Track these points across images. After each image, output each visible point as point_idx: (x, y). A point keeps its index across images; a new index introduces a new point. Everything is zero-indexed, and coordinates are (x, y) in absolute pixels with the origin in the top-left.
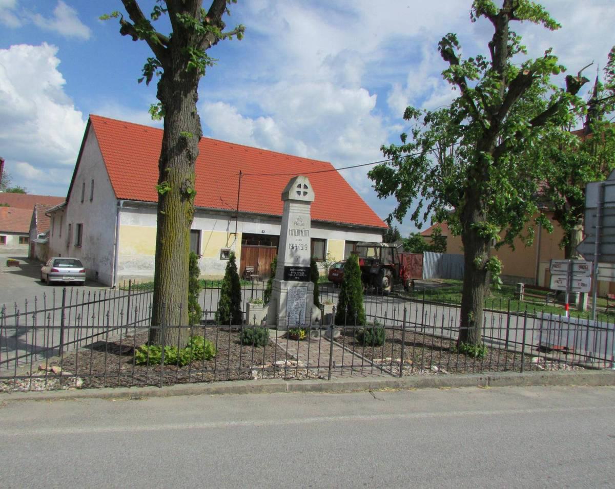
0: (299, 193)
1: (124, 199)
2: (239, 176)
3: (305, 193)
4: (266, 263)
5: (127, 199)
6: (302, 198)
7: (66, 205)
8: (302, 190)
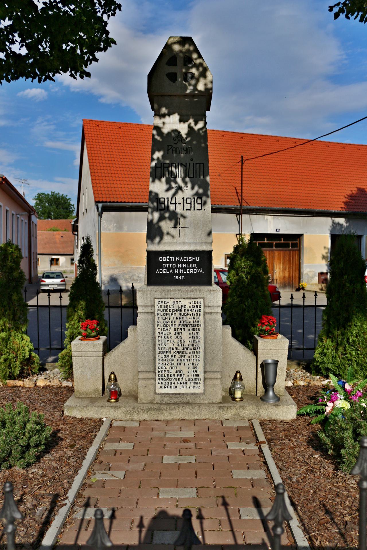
0: (173, 77)
1: (102, 202)
2: (240, 164)
4: (284, 269)
5: (106, 202)
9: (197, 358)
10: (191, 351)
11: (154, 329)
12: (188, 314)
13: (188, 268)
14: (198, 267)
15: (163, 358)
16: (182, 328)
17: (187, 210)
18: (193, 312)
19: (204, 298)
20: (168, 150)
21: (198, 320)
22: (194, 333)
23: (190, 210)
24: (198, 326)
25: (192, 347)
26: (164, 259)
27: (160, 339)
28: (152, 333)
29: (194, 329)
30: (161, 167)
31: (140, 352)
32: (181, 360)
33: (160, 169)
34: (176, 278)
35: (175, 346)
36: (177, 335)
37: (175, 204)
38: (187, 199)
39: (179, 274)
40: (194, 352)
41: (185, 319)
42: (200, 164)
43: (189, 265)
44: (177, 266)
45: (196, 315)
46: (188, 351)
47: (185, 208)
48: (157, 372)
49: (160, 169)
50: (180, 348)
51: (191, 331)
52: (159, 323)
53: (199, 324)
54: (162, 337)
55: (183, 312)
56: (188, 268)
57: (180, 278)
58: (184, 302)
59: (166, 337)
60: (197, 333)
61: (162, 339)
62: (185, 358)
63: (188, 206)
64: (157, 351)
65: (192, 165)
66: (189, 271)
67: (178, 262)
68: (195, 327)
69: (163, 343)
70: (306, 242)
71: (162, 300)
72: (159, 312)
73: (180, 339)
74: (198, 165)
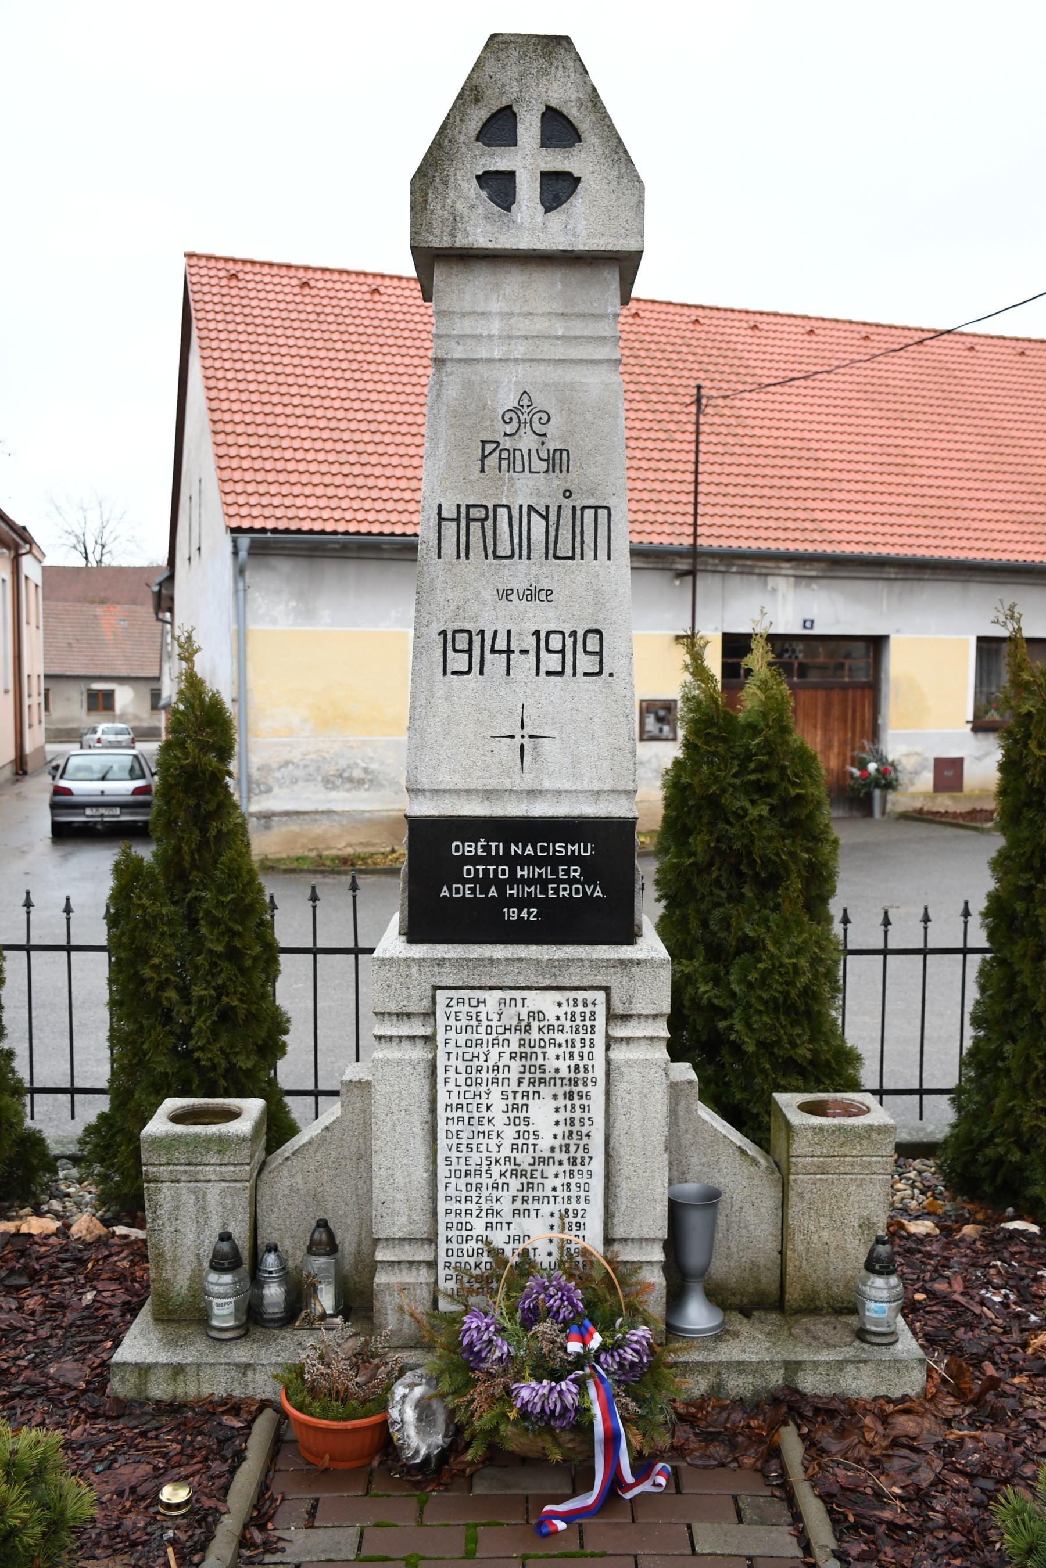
0: (500, 187)
2: (693, 409)
3: (558, 188)
6: (530, 226)
7: (171, 578)
8: (527, 159)
9: (582, 1194)
10: (561, 1169)
11: (433, 1101)
12: (553, 1042)
13: (552, 881)
14: (588, 878)
15: (464, 1194)
16: (531, 1089)
17: (548, 673)
18: (569, 1036)
19: (607, 989)
20: (484, 457)
21: (586, 1061)
22: (573, 1106)
23: (561, 673)
24: (585, 1084)
25: (564, 1157)
26: (469, 849)
27: (454, 1128)
28: (426, 1105)
29: (571, 1094)
30: (458, 520)
31: (383, 1172)
32: (524, 1200)
33: (454, 524)
34: (512, 914)
35: (506, 1151)
36: (512, 1115)
37: (509, 652)
38: (548, 634)
39: (521, 903)
40: (571, 1172)
41: (540, 1061)
42: (596, 508)
43: (555, 872)
44: (513, 872)
45: (578, 1044)
46: (551, 1170)
47: (543, 669)
48: (442, 1239)
49: (454, 524)
50: (524, 1160)
51: (561, 1102)
52: (451, 1074)
53: (590, 1075)
54: (460, 1120)
55: (535, 1035)
56: (552, 881)
57: (524, 914)
58: (536, 1000)
59: (474, 1122)
60: (583, 1108)
61: (460, 1127)
62: (540, 1194)
63: (552, 662)
64: (442, 1170)
65: (566, 514)
66: (556, 891)
67: (515, 861)
68: (572, 1088)
69: (465, 1141)
70: (898, 663)
71: (462, 993)
72: (452, 1034)
73: (522, 1128)
74: (589, 514)
